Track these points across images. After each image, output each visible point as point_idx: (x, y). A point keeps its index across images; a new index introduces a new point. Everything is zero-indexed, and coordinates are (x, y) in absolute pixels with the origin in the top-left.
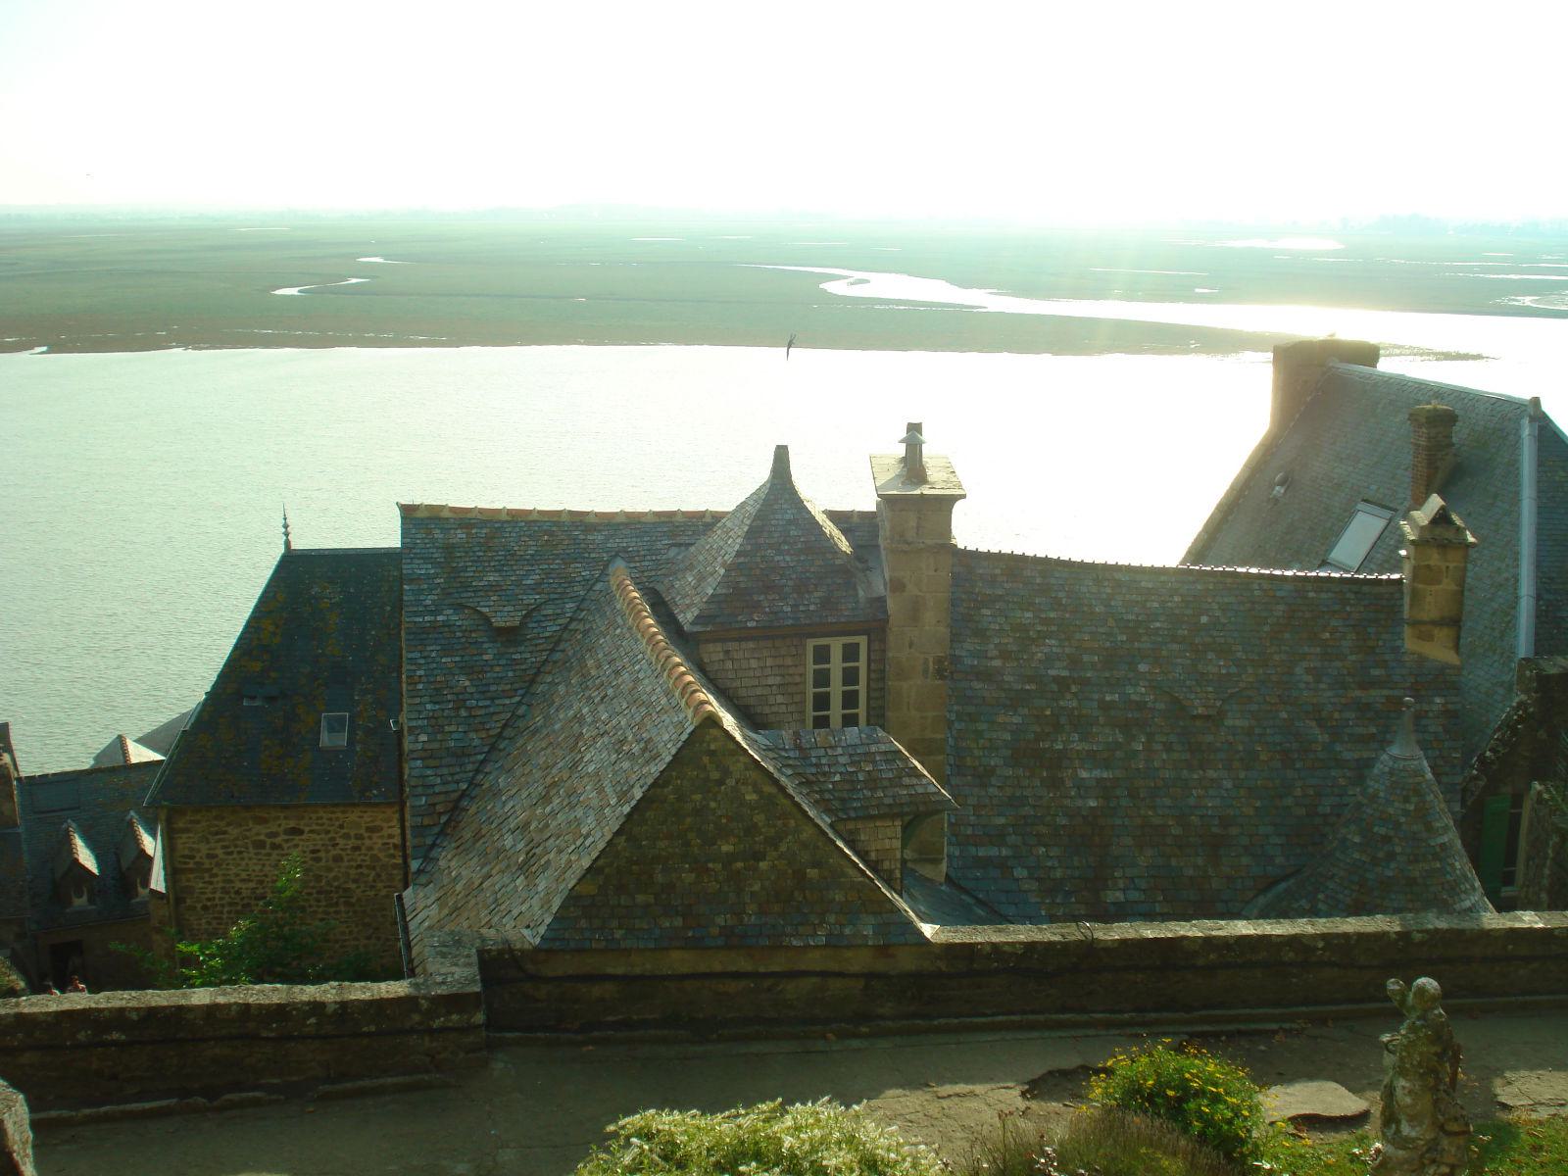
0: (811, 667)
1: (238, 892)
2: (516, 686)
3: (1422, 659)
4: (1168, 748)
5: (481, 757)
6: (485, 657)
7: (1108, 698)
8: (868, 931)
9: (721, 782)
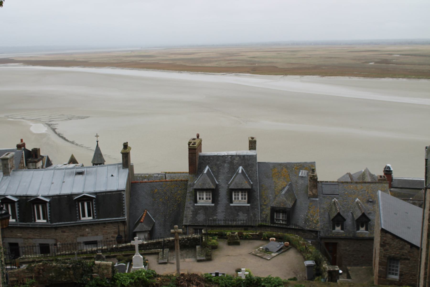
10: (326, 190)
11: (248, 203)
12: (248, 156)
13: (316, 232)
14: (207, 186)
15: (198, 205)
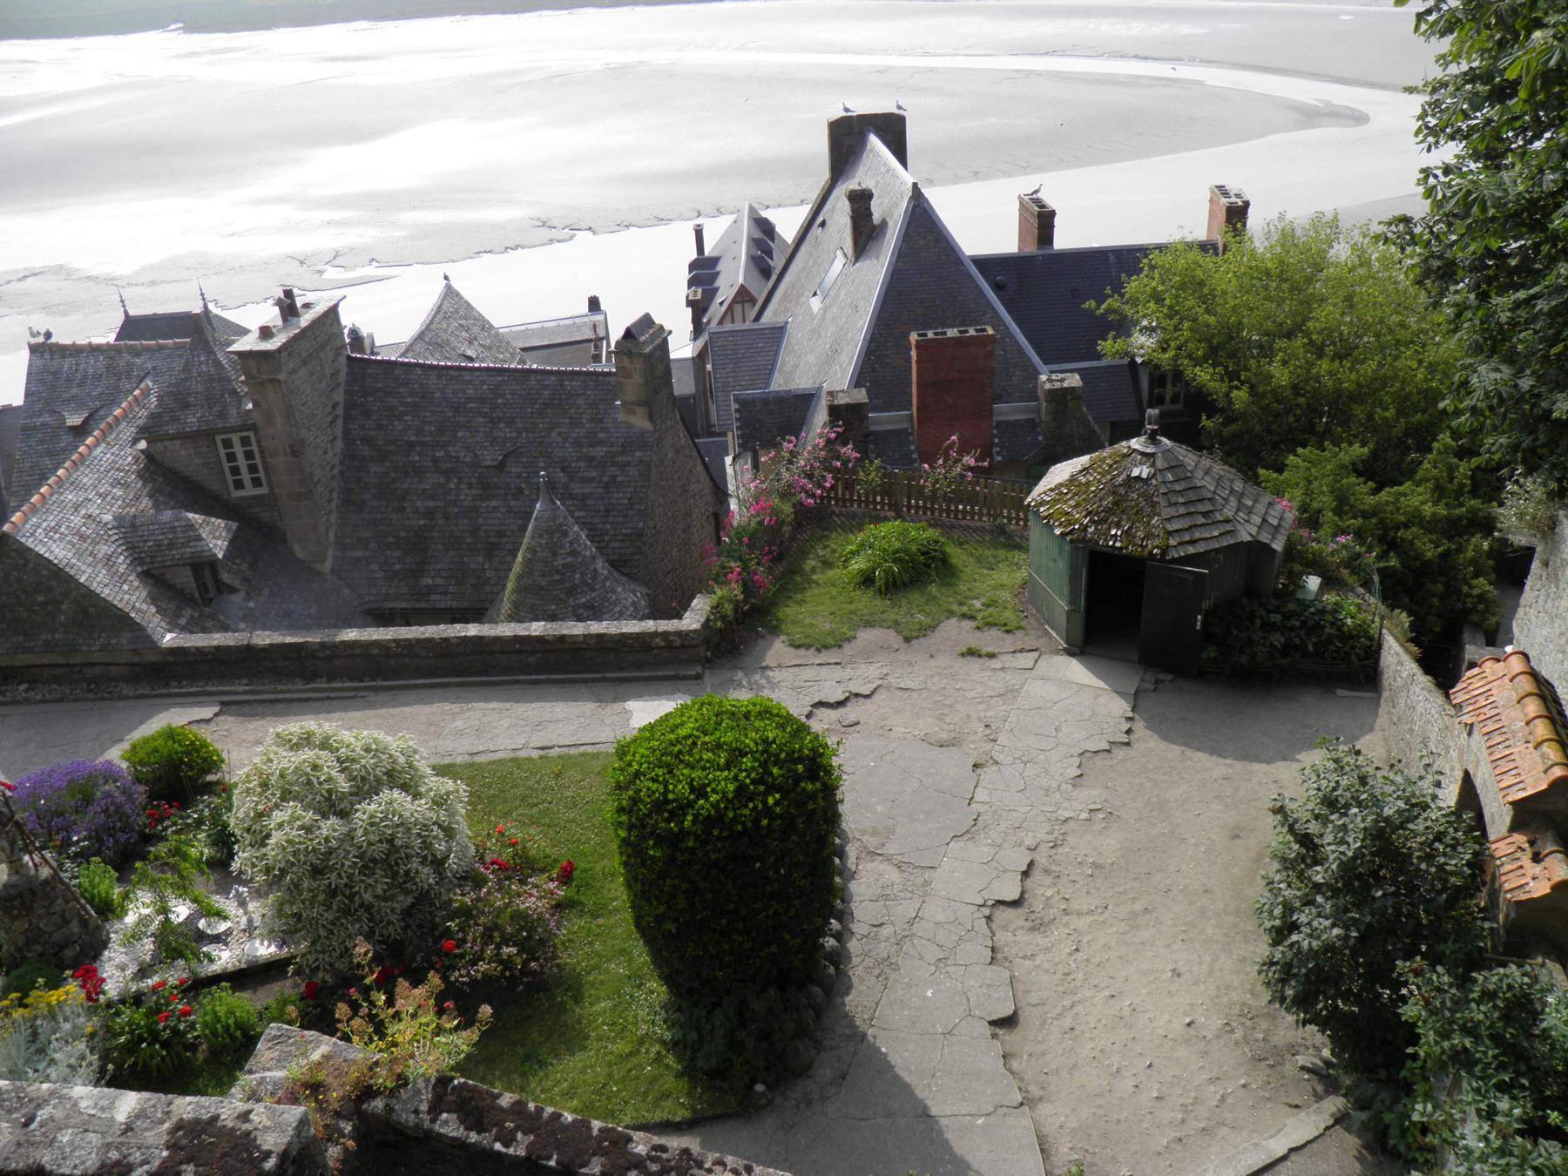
0: (222, 452)
3: (630, 426)
4: (470, 486)
7: (437, 454)
8: (124, 641)
9: (25, 565)
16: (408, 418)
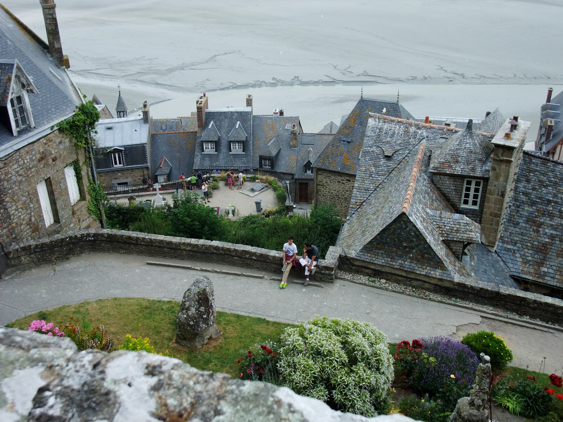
0: (465, 186)
1: (332, 193)
2: (386, 173)
5: (372, 192)
6: (380, 163)
9: (405, 228)
10: (305, 140)
11: (243, 152)
12: (244, 112)
13: (293, 175)
14: (211, 139)
15: (204, 153)
16: (550, 188)
